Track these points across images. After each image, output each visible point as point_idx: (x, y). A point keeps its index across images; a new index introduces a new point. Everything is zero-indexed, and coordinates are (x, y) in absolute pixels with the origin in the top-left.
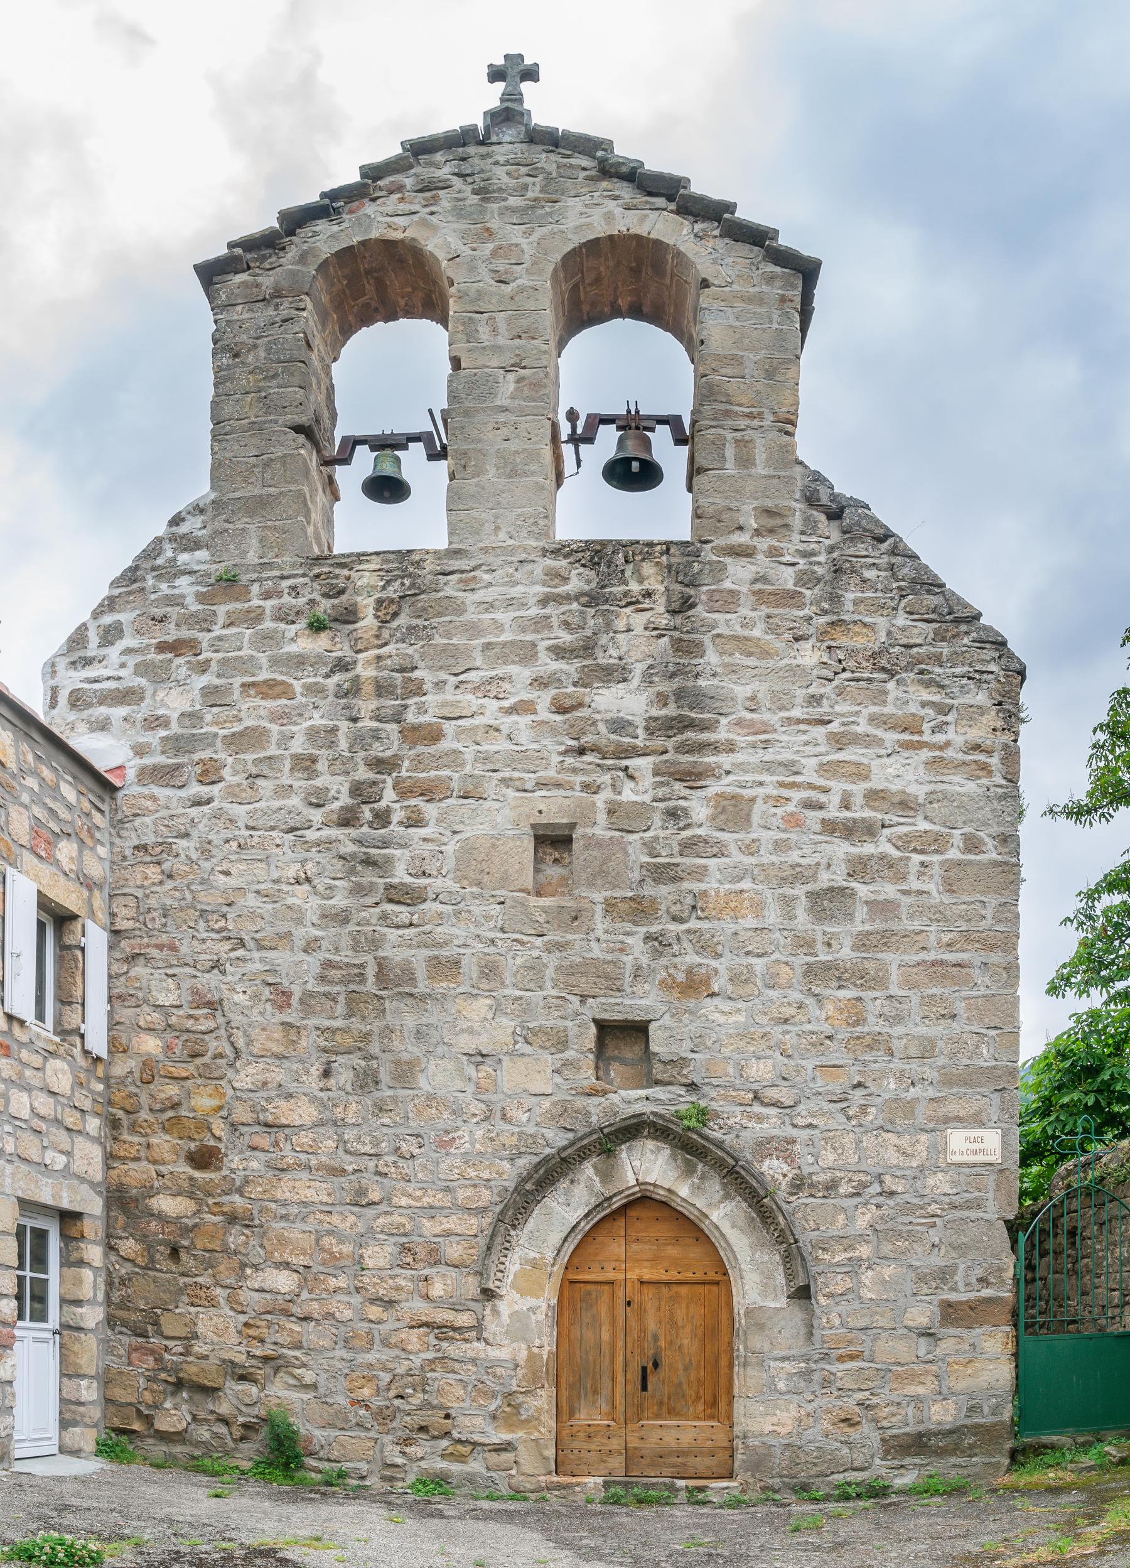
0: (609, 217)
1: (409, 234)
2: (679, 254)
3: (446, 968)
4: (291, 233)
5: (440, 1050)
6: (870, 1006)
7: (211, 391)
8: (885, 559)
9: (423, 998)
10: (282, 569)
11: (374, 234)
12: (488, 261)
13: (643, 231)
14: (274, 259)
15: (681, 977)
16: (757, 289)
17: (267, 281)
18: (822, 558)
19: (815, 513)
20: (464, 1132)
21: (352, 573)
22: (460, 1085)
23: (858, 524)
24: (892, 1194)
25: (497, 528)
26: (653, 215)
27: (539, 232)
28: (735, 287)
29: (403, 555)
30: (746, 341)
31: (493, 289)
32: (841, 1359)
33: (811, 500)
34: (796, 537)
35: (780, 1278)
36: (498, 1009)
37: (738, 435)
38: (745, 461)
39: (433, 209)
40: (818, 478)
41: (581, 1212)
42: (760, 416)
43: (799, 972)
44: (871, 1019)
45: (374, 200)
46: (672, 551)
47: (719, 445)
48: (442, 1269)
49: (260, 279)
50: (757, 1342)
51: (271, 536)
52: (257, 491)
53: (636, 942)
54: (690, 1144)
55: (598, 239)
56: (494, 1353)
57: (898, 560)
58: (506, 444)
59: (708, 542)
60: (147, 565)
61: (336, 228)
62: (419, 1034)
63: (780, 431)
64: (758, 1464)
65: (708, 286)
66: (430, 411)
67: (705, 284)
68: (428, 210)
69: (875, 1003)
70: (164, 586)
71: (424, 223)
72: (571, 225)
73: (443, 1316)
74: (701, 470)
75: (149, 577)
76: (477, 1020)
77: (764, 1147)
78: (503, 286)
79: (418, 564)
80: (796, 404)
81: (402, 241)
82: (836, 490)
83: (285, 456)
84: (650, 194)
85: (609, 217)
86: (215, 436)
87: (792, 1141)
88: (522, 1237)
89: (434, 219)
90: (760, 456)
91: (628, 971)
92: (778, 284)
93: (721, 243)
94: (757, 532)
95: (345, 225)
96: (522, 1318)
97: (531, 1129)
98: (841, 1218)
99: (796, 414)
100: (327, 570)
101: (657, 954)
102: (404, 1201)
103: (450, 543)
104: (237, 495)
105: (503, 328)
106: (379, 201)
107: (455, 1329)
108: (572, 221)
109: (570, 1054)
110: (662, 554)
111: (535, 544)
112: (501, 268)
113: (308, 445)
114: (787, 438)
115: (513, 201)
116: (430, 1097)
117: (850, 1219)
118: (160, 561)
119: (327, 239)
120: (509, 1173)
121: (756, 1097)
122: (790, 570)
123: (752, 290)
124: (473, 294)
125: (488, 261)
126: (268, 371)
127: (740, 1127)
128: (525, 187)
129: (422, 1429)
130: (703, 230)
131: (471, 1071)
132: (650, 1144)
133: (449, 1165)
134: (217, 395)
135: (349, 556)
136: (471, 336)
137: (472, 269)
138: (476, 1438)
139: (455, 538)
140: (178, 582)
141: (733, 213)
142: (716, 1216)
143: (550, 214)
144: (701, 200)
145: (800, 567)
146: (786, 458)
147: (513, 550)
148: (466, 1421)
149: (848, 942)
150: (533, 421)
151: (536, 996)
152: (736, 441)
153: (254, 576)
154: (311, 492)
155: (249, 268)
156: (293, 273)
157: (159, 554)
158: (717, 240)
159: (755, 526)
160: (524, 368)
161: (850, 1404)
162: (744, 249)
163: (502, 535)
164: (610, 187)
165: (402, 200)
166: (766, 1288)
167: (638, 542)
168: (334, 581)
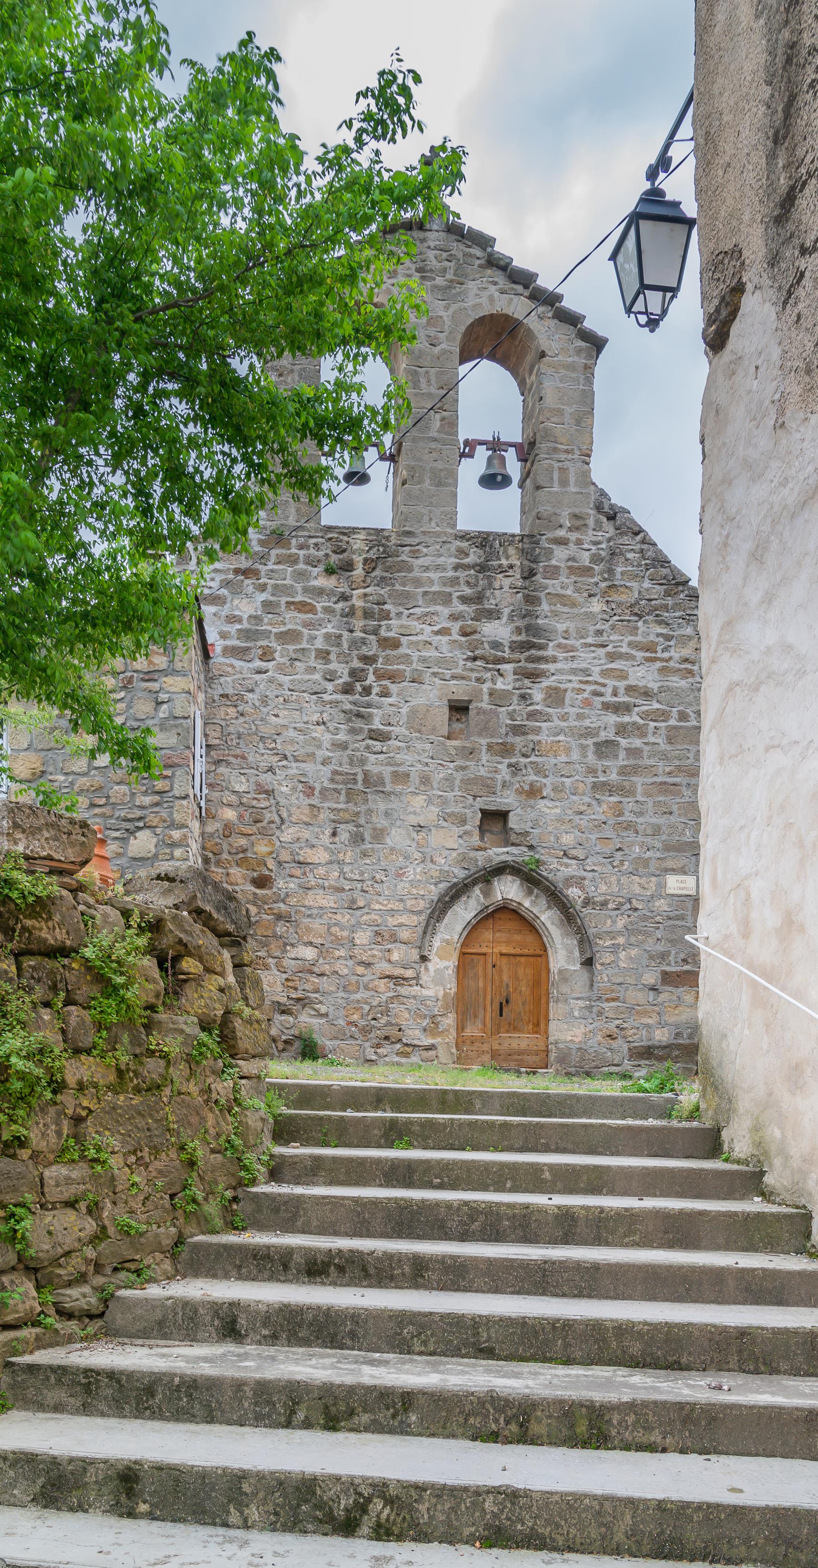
0: (491, 299)
3: (401, 777)
5: (398, 823)
6: (625, 806)
8: (638, 547)
9: (389, 794)
15: (527, 788)
18: (603, 546)
20: (410, 869)
22: (409, 842)
24: (636, 909)
32: (607, 1000)
34: (591, 532)
35: (577, 954)
36: (429, 801)
41: (473, 914)
43: (589, 786)
44: (627, 813)
48: (398, 945)
50: (565, 989)
53: (503, 767)
54: (531, 878)
56: (426, 992)
57: (645, 547)
58: (435, 464)
62: (387, 814)
64: (563, 1059)
69: (629, 804)
73: (398, 972)
76: (418, 807)
77: (569, 881)
85: (491, 299)
87: (584, 879)
88: (441, 927)
91: (499, 783)
94: (570, 529)
97: (446, 868)
98: (609, 922)
101: (514, 774)
102: (377, 907)
107: (404, 979)
108: (470, 302)
109: (467, 827)
116: (392, 849)
117: (614, 922)
120: (434, 892)
121: (565, 854)
127: (558, 870)
129: (387, 1038)
131: (414, 835)
132: (510, 878)
133: (402, 887)
138: (416, 1042)
142: (543, 918)
143: (459, 294)
147: (438, 535)
148: (410, 1032)
149: (615, 771)
151: (450, 795)
161: (612, 1026)
163: (433, 524)
166: (569, 959)
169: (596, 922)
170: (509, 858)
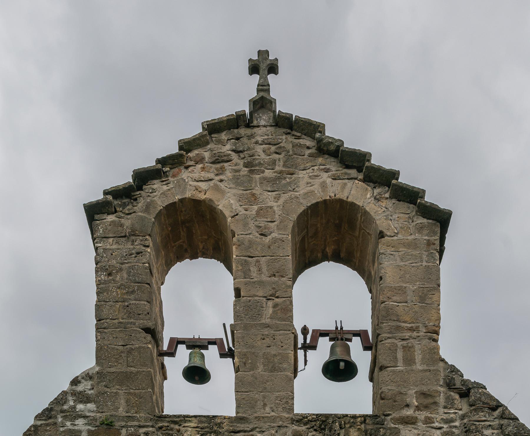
0: (323, 185)
1: (208, 196)
2: (366, 213)
4: (140, 188)
7: (95, 298)
8: (497, 422)
10: (139, 421)
11: (188, 195)
12: (255, 219)
13: (343, 196)
14: (130, 207)
16: (413, 237)
17: (127, 222)
18: (457, 424)
19: (452, 393)
21: (181, 427)
23: (479, 399)
25: (265, 405)
26: (349, 183)
27: (284, 197)
28: (400, 236)
29: (211, 419)
30: (408, 276)
31: (258, 240)
33: (450, 385)
34: (441, 410)
37: (405, 343)
38: (409, 361)
39: (222, 177)
40: (454, 370)
42: (417, 329)
45: (187, 168)
46: (367, 421)
47: (393, 350)
49: (123, 221)
51: (133, 399)
52: (123, 369)
55: (317, 203)
57: (505, 422)
58: (268, 350)
59: (388, 415)
60: (58, 408)
61: (165, 188)
63: (430, 339)
65: (383, 237)
66: (224, 325)
67: (382, 235)
68: (218, 178)
70: (68, 423)
71: (216, 188)
72: (301, 192)
74: (382, 368)
75: (59, 416)
78: (264, 238)
79: (219, 425)
80: (439, 319)
81: (204, 201)
82: (465, 377)
83: (140, 347)
84: (348, 167)
85: (323, 185)
86: (98, 328)
89: (221, 185)
90: (418, 357)
92: (425, 232)
93: (389, 203)
94: (418, 408)
95: (171, 186)
99: (439, 327)
100: (166, 424)
103: (237, 413)
104: (112, 370)
105: (264, 269)
106: (190, 169)
108: (302, 190)
110: (361, 423)
111: (287, 416)
112: (262, 225)
113: (153, 342)
114: (434, 344)
115: (268, 173)
118: (65, 407)
119: (161, 194)
122: (438, 432)
123: (409, 238)
124: (246, 243)
125: (255, 219)
126: (129, 288)
128: (274, 162)
130: (379, 194)
134: (99, 301)
135: (179, 416)
136: (246, 274)
137: (246, 225)
139: (240, 410)
140: (77, 422)
141: (397, 179)
143: (289, 184)
144: (378, 170)
145: (445, 430)
146: (434, 356)
147: (273, 419)
150: (284, 334)
152: (404, 347)
153: (123, 424)
154: (154, 373)
155: (116, 211)
156: (142, 219)
157: (65, 403)
158: (387, 201)
159: (416, 404)
160: (278, 297)
162: (404, 207)
163: (268, 409)
164: (324, 162)
165: (203, 169)
167: (347, 416)
168: (171, 432)
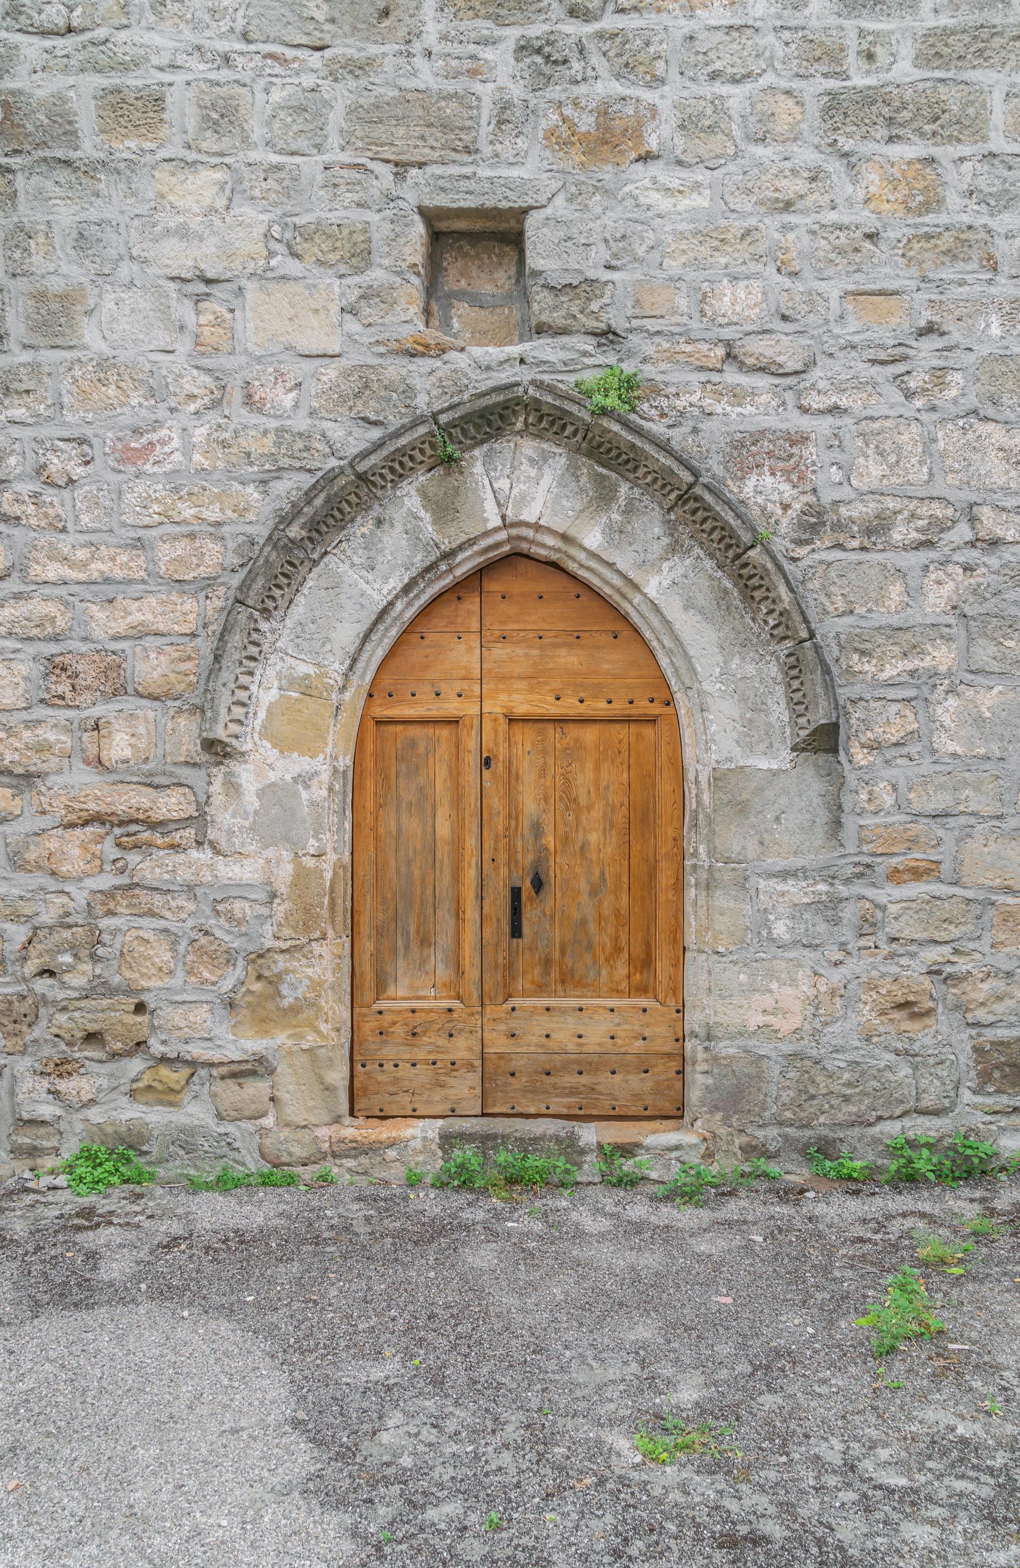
3: (135, 109)
5: (126, 271)
6: (950, 174)
9: (91, 169)
15: (586, 123)
20: (170, 433)
22: (162, 338)
32: (895, 876)
35: (779, 711)
36: (234, 191)
41: (396, 583)
43: (814, 108)
44: (953, 200)
50: (735, 839)
54: (606, 445)
62: (82, 240)
69: (959, 170)
76: (196, 208)
87: (801, 439)
88: (282, 633)
91: (487, 111)
96: (284, 792)
97: (301, 423)
98: (896, 591)
101: (541, 80)
109: (376, 276)
116: (104, 364)
117: (914, 593)
120: (257, 509)
121: (730, 356)
127: (704, 414)
131: (186, 312)
132: (529, 447)
133: (142, 497)
142: (653, 586)
149: (907, 50)
151: (311, 166)
166: (750, 733)
169: (840, 592)
170: (525, 375)
